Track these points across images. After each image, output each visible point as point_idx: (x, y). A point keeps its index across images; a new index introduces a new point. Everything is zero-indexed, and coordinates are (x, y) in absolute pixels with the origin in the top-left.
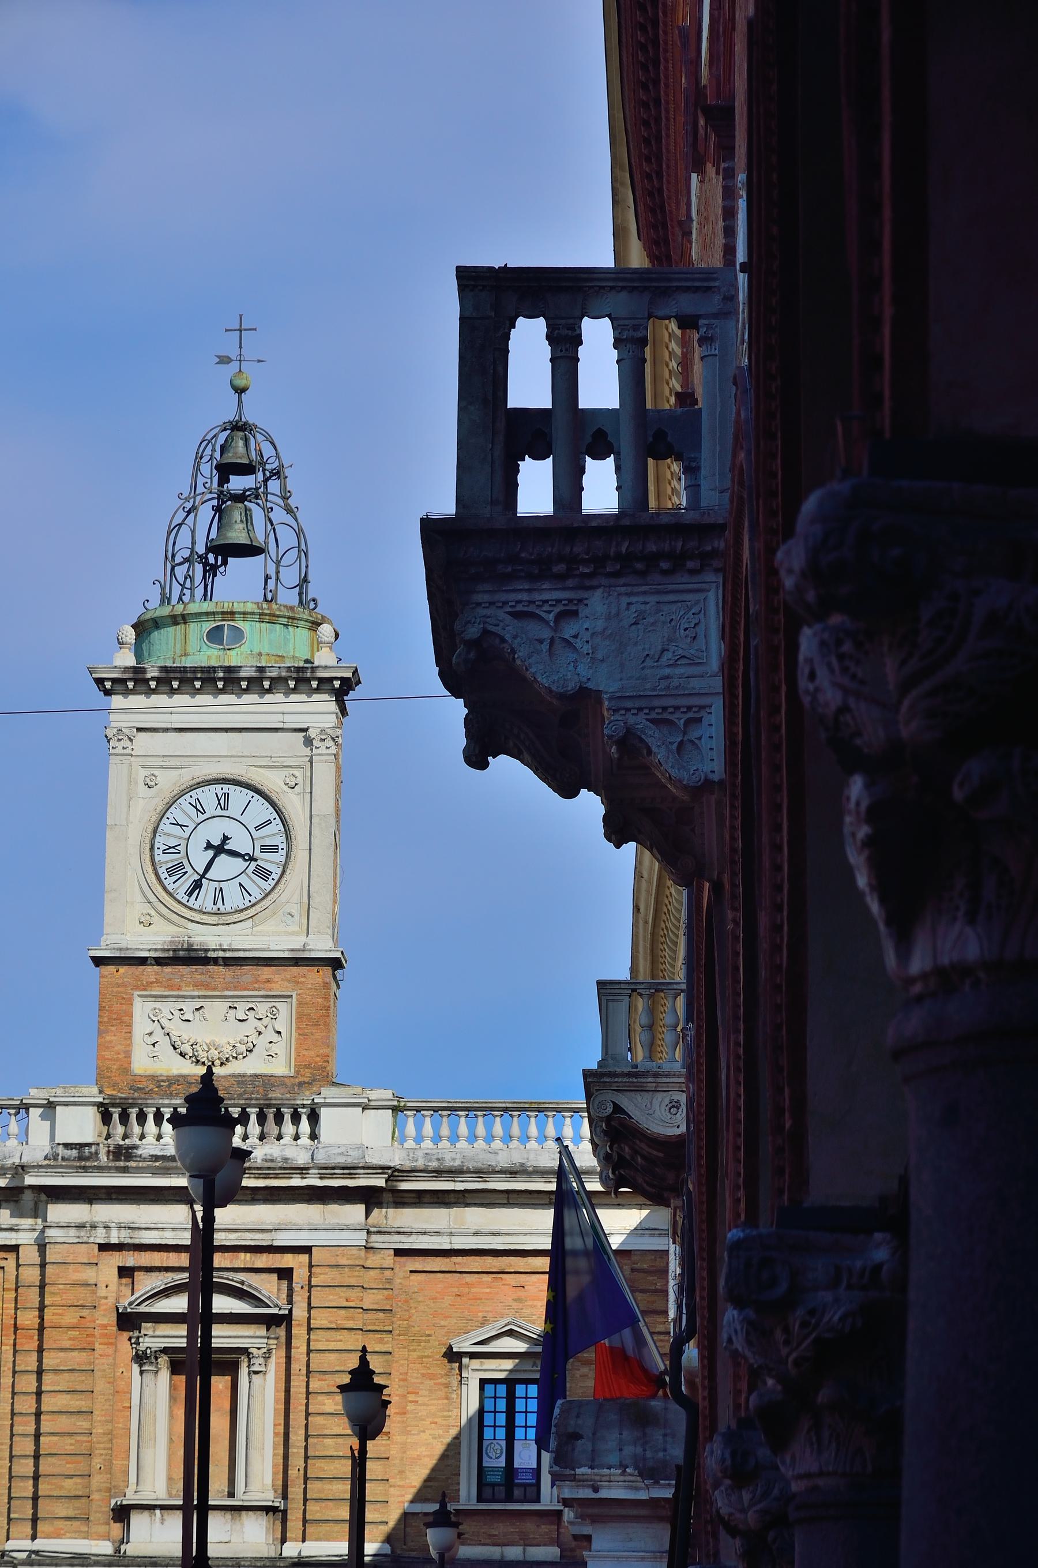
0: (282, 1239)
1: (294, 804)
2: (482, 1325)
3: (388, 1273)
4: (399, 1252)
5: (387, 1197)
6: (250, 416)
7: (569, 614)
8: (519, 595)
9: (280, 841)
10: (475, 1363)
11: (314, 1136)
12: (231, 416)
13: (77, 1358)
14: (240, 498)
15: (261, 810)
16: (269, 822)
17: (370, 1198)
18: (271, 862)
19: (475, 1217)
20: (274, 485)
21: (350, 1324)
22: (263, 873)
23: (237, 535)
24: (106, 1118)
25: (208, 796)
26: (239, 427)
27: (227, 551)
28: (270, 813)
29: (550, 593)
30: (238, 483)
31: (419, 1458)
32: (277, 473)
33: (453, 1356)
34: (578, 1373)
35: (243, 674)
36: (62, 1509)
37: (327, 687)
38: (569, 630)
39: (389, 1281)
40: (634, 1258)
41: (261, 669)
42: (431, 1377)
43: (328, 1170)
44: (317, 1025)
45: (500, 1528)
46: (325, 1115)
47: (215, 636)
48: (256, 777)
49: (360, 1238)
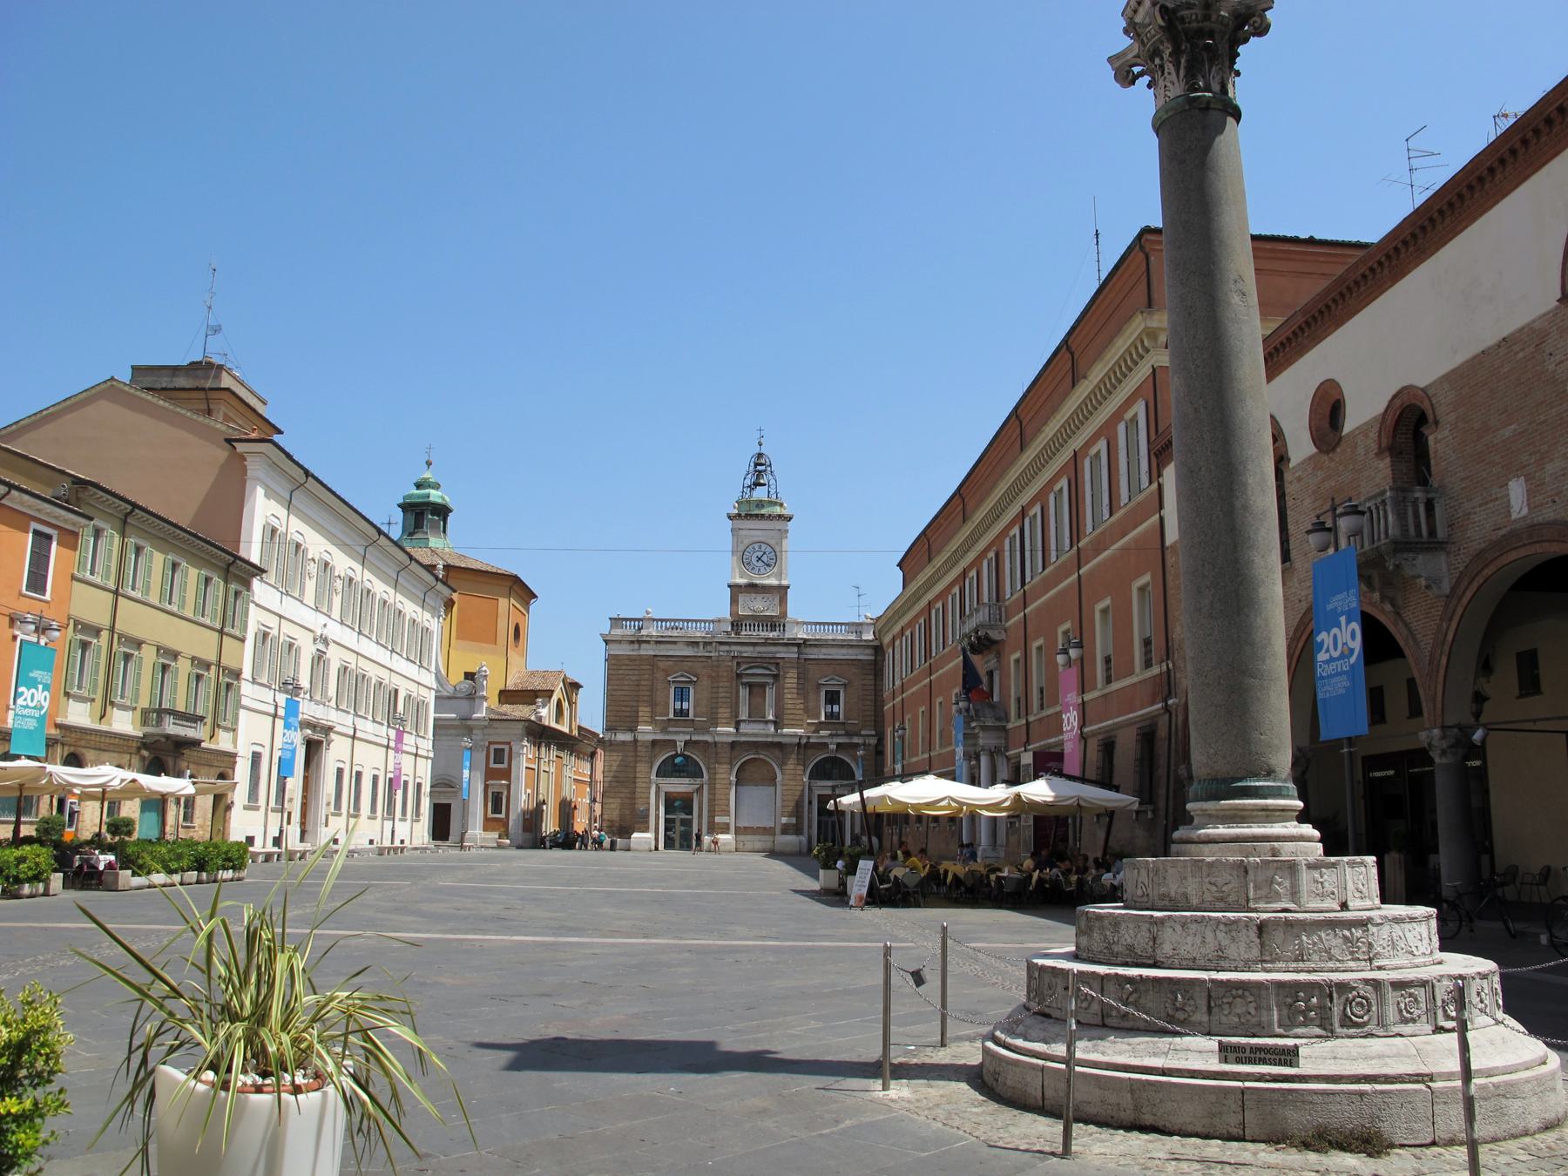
0: (778, 655)
1: (777, 550)
6: (763, 451)
7: (1414, 559)
8: (1405, 556)
12: (758, 451)
13: (727, 684)
14: (760, 472)
15: (769, 549)
18: (772, 562)
19: (824, 650)
20: (769, 469)
23: (762, 481)
24: (732, 625)
25: (756, 546)
26: (760, 455)
27: (757, 484)
29: (1411, 555)
30: (759, 468)
32: (770, 465)
33: (819, 685)
36: (724, 721)
38: (1415, 562)
43: (789, 639)
47: (757, 506)
48: (768, 541)
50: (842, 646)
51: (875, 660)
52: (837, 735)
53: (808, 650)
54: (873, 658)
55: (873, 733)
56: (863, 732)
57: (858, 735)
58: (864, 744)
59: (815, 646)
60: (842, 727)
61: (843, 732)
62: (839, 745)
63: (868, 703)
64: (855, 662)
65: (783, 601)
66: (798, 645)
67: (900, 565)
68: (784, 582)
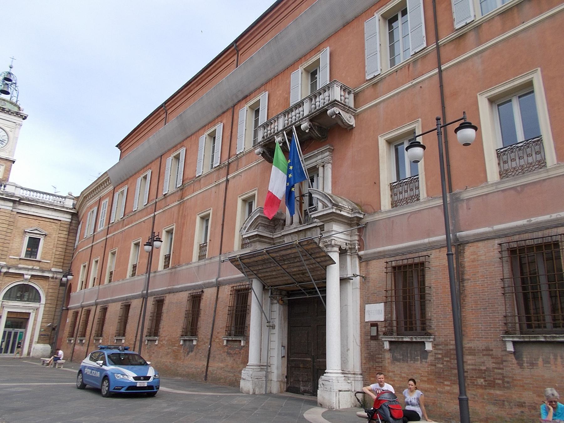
1: (10, 134)
2: (31, 227)
3: (15, 216)
4: (18, 213)
5: (17, 202)
6: (12, 72)
9: (7, 139)
10: (29, 234)
11: (4, 190)
16: (5, 136)
17: (14, 202)
21: (6, 223)
22: (2, 144)
23: (6, 89)
28: (5, 134)
31: (14, 248)
34: (48, 238)
35: (6, 110)
37: (21, 117)
39: (15, 217)
40: (62, 221)
41: (10, 110)
42: (20, 235)
43: (7, 195)
44: (8, 171)
45: (28, 262)
46: (7, 186)
49: (11, 209)
50: (49, 209)
51: (71, 222)
52: (32, 269)
53: (21, 207)
54: (70, 220)
55: (61, 271)
56: (53, 269)
57: (50, 271)
58: (53, 278)
59: (27, 205)
60: (37, 263)
61: (38, 268)
62: (33, 276)
63: (60, 249)
64: (56, 222)
65: (8, 171)
66: (14, 202)
67: (119, 146)
68: (11, 158)
